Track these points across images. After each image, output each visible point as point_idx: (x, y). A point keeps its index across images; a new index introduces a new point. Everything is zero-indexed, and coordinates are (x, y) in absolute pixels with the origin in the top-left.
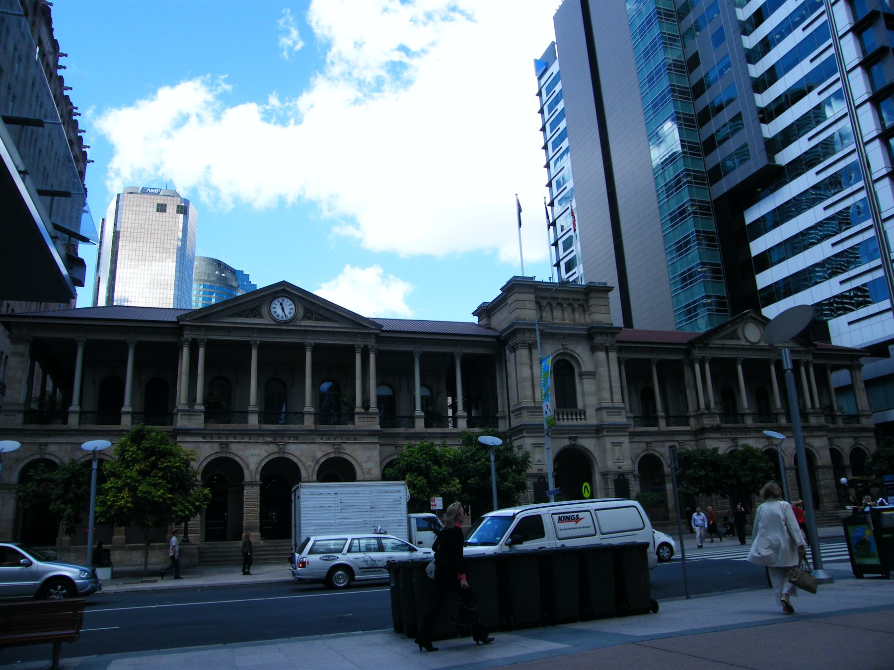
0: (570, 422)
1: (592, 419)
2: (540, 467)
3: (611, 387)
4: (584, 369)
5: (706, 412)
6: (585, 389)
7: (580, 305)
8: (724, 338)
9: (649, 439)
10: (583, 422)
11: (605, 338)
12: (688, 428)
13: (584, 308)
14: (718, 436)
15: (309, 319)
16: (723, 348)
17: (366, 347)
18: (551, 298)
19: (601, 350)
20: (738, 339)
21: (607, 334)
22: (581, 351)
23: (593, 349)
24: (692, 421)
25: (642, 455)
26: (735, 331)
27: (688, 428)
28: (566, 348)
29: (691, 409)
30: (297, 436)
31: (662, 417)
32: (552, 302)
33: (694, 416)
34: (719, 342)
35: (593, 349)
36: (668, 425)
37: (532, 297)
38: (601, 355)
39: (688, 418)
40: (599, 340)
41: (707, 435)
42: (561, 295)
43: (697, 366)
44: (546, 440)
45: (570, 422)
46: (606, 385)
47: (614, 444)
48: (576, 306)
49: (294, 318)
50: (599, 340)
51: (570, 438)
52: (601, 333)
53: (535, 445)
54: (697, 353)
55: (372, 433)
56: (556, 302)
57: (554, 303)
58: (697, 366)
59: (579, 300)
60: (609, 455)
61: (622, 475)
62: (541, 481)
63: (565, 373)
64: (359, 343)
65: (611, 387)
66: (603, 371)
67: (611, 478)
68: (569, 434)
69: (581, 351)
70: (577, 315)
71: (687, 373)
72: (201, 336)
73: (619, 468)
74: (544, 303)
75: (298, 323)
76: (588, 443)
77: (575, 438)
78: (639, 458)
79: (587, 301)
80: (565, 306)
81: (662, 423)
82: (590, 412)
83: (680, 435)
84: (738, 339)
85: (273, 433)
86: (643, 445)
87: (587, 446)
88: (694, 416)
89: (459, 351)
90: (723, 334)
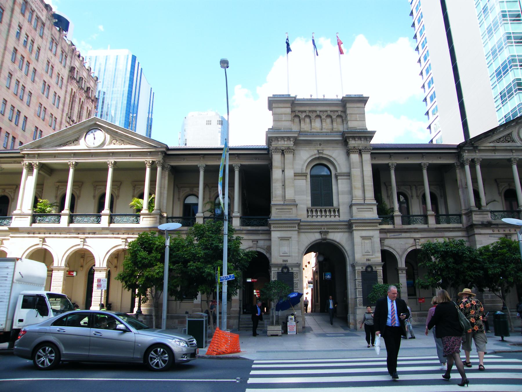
0: (324, 219)
1: (344, 216)
2: (285, 258)
3: (363, 186)
4: (339, 171)
5: (477, 209)
6: (340, 189)
7: (339, 116)
8: (498, 141)
10: (337, 218)
11: (359, 142)
12: (460, 225)
14: (489, 231)
15: (114, 144)
16: (495, 150)
17: (153, 162)
18: (310, 111)
19: (354, 152)
20: (513, 141)
21: (360, 138)
22: (336, 154)
24: (464, 218)
25: (409, 250)
26: (510, 135)
27: (460, 225)
28: (322, 153)
29: (463, 208)
30: (94, 232)
31: (432, 215)
32: (310, 114)
33: (465, 214)
34: (492, 144)
35: (348, 153)
36: (438, 222)
37: (289, 110)
38: (355, 157)
39: (460, 215)
40: (352, 143)
41: (476, 231)
42: (319, 108)
43: (467, 167)
44: (294, 235)
45: (324, 219)
46: (357, 184)
47: (364, 238)
48: (334, 117)
49: (103, 144)
50: (352, 143)
51: (321, 233)
52: (354, 138)
53: (282, 239)
54: (467, 156)
56: (315, 114)
57: (313, 115)
58: (467, 167)
59: (337, 111)
60: (357, 249)
61: (370, 266)
62: (285, 271)
65: (363, 186)
66: (356, 172)
67: (358, 268)
68: (321, 229)
69: (336, 154)
70: (335, 124)
71: (459, 175)
72: (36, 162)
73: (368, 260)
74: (303, 116)
75: (105, 147)
76: (338, 237)
77: (327, 232)
78: (406, 253)
79: (344, 112)
80: (323, 117)
81: (432, 221)
82: (344, 209)
83: (451, 231)
84: (513, 141)
85: (78, 231)
86: (412, 241)
87: (338, 240)
88: (465, 214)
90: (495, 138)
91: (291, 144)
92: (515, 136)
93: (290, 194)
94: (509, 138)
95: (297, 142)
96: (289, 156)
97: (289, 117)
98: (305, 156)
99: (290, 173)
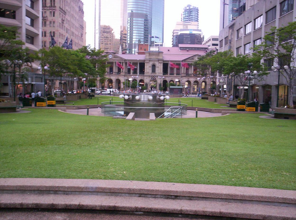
1: (157, 75)
8: (190, 59)
9: (172, 77)
13: (158, 55)
23: (159, 63)
34: (189, 60)
36: (176, 75)
37: (148, 54)
38: (160, 64)
50: (160, 61)
55: (123, 75)
63: (154, 66)
64: (122, 61)
66: (160, 67)
82: (157, 73)
89: (138, 62)
91: (148, 61)
92: (194, 58)
93: (148, 71)
94: (193, 59)
95: (150, 61)
96: (148, 64)
97: (148, 56)
98: (151, 63)
99: (148, 67)
